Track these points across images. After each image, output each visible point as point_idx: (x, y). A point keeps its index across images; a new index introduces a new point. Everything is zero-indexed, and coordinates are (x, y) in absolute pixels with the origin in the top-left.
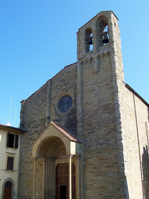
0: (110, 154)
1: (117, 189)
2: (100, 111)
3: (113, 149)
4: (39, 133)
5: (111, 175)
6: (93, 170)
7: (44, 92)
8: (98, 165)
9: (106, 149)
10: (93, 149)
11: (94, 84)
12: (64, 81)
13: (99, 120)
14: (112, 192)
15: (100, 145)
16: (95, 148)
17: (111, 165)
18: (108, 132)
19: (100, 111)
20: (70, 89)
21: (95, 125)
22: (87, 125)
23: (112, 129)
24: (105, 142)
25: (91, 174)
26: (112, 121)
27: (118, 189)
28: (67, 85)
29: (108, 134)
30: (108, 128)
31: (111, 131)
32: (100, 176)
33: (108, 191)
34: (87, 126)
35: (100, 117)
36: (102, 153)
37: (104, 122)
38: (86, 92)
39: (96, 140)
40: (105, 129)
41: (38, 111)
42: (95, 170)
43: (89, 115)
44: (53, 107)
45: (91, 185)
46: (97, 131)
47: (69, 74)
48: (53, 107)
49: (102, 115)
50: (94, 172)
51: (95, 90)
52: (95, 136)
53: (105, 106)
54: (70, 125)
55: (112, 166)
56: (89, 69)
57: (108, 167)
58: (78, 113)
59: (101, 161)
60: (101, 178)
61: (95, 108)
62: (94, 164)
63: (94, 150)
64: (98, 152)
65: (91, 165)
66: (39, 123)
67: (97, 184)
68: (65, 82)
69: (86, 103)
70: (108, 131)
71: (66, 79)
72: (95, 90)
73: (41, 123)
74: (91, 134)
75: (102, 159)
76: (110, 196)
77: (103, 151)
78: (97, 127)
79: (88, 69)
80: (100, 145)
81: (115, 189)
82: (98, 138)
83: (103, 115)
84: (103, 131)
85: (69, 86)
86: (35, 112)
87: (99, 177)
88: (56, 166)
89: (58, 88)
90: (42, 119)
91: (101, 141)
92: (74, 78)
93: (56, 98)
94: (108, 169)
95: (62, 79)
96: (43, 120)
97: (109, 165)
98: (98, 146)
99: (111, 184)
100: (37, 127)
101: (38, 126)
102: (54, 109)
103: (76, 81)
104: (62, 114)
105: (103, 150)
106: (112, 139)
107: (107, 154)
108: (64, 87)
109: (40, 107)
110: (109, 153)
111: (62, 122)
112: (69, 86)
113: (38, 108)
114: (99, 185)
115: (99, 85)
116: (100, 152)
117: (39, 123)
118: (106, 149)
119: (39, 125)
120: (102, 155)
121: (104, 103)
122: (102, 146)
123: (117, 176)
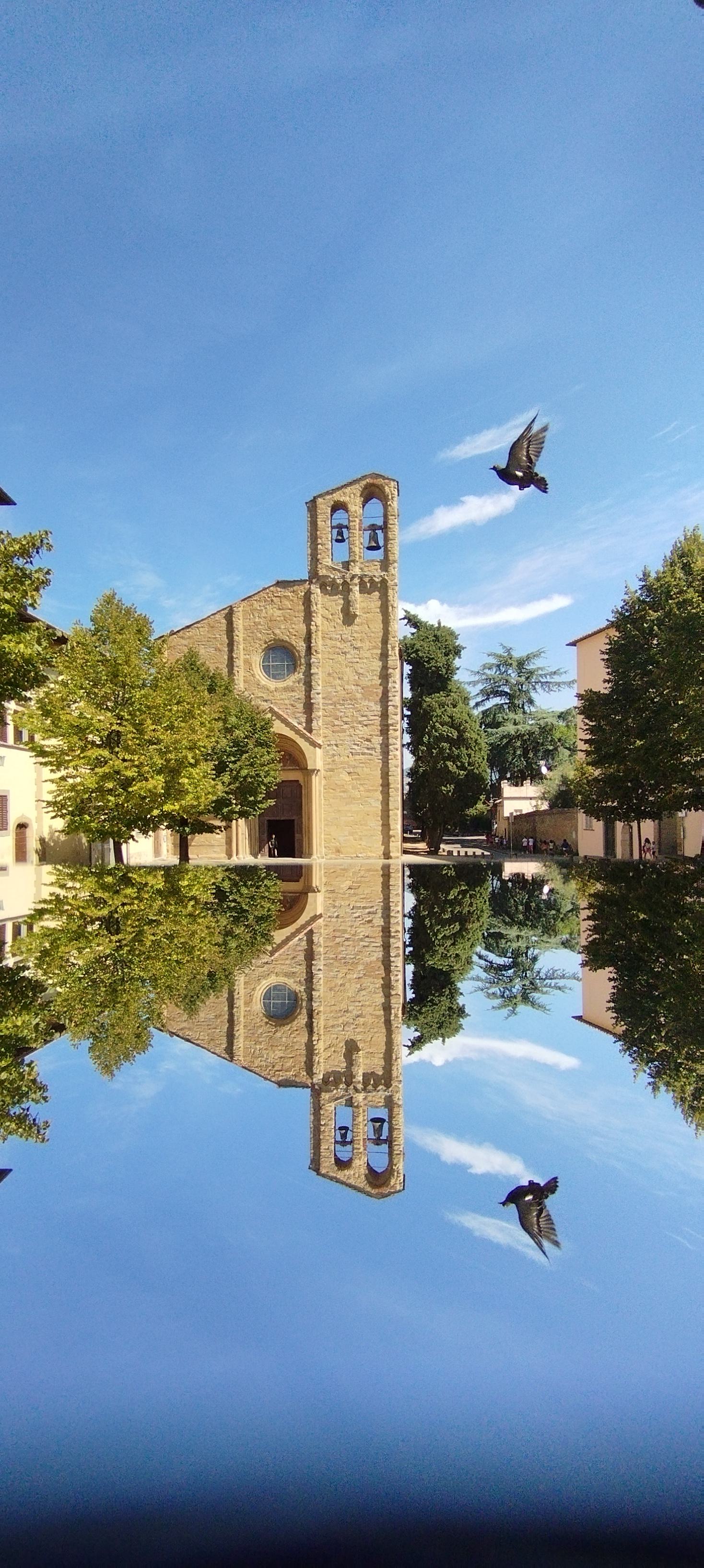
6: (342, 794)
17: (375, 788)
32: (354, 804)
50: (344, 798)
52: (348, 738)
53: (368, 687)
57: (369, 791)
71: (281, 612)
72: (348, 652)
74: (339, 734)
75: (359, 779)
77: (361, 765)
79: (334, 603)
104: (272, 684)
116: (357, 767)
122: (357, 757)
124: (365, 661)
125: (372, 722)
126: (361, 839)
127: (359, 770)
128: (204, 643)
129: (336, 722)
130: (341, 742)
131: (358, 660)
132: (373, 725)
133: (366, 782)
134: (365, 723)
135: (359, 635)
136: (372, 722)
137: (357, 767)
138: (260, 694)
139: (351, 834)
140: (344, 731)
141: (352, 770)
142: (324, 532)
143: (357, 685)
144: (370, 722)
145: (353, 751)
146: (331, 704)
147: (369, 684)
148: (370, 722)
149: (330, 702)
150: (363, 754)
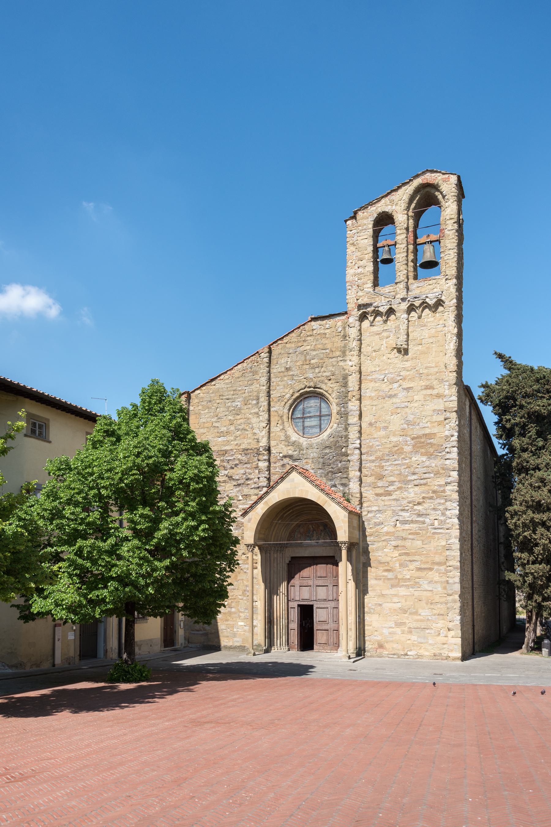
0: (426, 544)
1: (438, 615)
2: (407, 449)
3: (434, 533)
4: (239, 482)
5: (426, 587)
6: (386, 574)
7: (247, 379)
8: (398, 565)
9: (418, 534)
10: (386, 529)
11: (393, 381)
12: (308, 357)
13: (403, 467)
14: (428, 619)
15: (405, 522)
16: (392, 529)
18: (423, 498)
19: (407, 449)
20: (326, 381)
21: (392, 479)
22: (371, 475)
23: (434, 492)
24: (415, 518)
25: (381, 582)
26: (435, 475)
27: (441, 615)
28: (317, 370)
29: (424, 502)
30: (423, 488)
31: (432, 495)
33: (419, 617)
34: (373, 478)
35: (407, 461)
36: (407, 540)
37: (414, 474)
38: (371, 398)
39: (394, 511)
40: (416, 489)
41: (232, 428)
42: (390, 575)
43: (379, 454)
44: (279, 422)
45: (380, 605)
46: (396, 493)
47: (324, 341)
48: (279, 422)
49: (411, 458)
50: (388, 579)
51: (395, 395)
52: (393, 503)
53: (419, 437)
54: (328, 473)
55: (431, 569)
56: (381, 339)
57: (419, 569)
58: (351, 446)
59: (404, 557)
60: (402, 591)
61: (394, 439)
62: (388, 563)
63: (388, 533)
64: (397, 538)
65: (381, 563)
66: (240, 457)
67: (395, 603)
68: (312, 361)
69: (371, 424)
70: (424, 495)
71: (314, 353)
72: (395, 395)
73: (244, 458)
74: (383, 498)
75: (407, 554)
76: (423, 627)
77: (410, 537)
78: (396, 483)
79: (377, 337)
80: (405, 522)
81: (434, 615)
82: (399, 508)
83: (414, 459)
84: (413, 493)
85: (325, 374)
86: (224, 429)
87: (399, 589)
88: (287, 562)
89: (291, 373)
90: (247, 450)
91: (406, 515)
92: (338, 353)
93: (286, 401)
94: (419, 574)
95: (302, 349)
96: (249, 451)
97: (423, 566)
98: (398, 525)
99: (427, 604)
100: (232, 468)
101: (236, 465)
102: (281, 427)
103: (341, 364)
104: (304, 442)
105: (409, 534)
106: (432, 512)
107: (419, 543)
108: (311, 376)
109: (238, 417)
110: (423, 541)
111: (307, 462)
112: (325, 374)
113: (230, 418)
114: (399, 605)
115: (406, 385)
116: (405, 539)
117: (240, 457)
118: (418, 534)
119: (237, 462)
120: (408, 543)
121: (417, 431)
122: (407, 526)
123: (440, 589)
124: (416, 405)
125: (424, 481)
126: (410, 632)
127: (408, 543)
128: (227, 397)
129: (380, 484)
130: (385, 508)
131: (406, 404)
132: (425, 484)
133: (416, 558)
134: (416, 482)
135: (408, 373)
136: (424, 481)
137: (405, 539)
138: (290, 452)
139: (399, 624)
140: (389, 494)
141: (399, 543)
142: (366, 252)
143: (406, 436)
144: (422, 482)
145: (401, 519)
146: (373, 461)
147: (421, 433)
148: (422, 482)
149: (373, 458)
150: (412, 522)
